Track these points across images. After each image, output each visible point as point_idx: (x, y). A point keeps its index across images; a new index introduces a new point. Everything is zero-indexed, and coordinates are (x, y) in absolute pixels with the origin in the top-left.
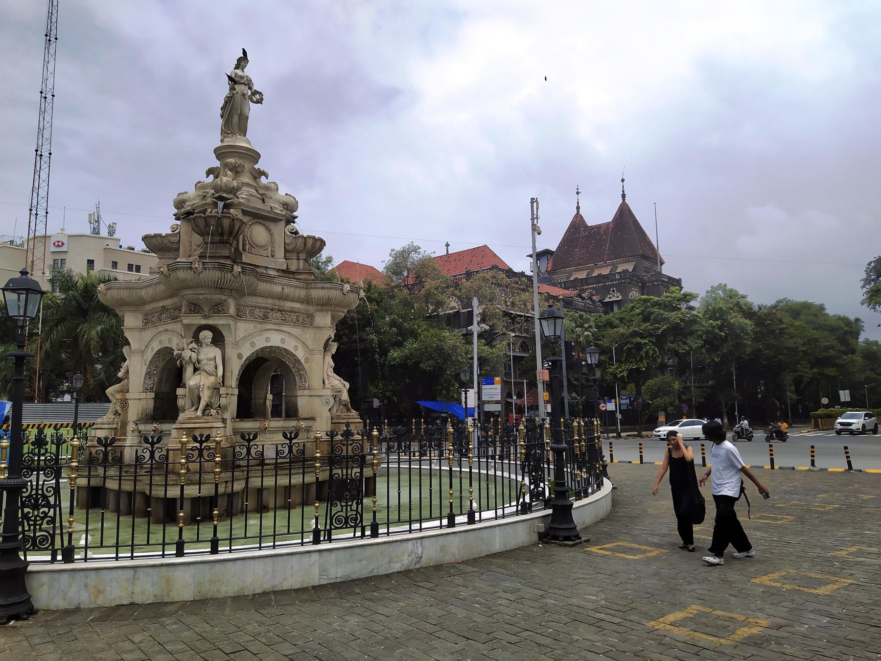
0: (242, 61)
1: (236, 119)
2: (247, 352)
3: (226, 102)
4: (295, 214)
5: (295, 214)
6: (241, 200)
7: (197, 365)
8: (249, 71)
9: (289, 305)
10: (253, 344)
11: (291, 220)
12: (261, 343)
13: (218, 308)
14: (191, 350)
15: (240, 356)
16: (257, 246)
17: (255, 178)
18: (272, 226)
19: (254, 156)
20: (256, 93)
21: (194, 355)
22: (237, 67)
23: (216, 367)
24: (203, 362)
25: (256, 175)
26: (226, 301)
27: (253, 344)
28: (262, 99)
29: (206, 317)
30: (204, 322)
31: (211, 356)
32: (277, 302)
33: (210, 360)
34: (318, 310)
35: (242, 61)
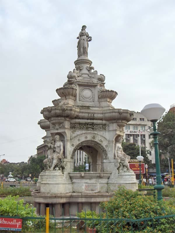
0: (84, 27)
1: (82, 50)
3: (78, 44)
4: (104, 82)
5: (104, 82)
7: (54, 149)
8: (87, 30)
9: (95, 121)
11: (103, 84)
12: (83, 139)
16: (86, 98)
17: (89, 71)
18: (92, 89)
21: (52, 146)
22: (82, 30)
23: (60, 150)
24: (56, 148)
25: (89, 69)
28: (91, 39)
30: (57, 131)
31: (58, 145)
33: (58, 147)
34: (110, 123)
35: (84, 27)
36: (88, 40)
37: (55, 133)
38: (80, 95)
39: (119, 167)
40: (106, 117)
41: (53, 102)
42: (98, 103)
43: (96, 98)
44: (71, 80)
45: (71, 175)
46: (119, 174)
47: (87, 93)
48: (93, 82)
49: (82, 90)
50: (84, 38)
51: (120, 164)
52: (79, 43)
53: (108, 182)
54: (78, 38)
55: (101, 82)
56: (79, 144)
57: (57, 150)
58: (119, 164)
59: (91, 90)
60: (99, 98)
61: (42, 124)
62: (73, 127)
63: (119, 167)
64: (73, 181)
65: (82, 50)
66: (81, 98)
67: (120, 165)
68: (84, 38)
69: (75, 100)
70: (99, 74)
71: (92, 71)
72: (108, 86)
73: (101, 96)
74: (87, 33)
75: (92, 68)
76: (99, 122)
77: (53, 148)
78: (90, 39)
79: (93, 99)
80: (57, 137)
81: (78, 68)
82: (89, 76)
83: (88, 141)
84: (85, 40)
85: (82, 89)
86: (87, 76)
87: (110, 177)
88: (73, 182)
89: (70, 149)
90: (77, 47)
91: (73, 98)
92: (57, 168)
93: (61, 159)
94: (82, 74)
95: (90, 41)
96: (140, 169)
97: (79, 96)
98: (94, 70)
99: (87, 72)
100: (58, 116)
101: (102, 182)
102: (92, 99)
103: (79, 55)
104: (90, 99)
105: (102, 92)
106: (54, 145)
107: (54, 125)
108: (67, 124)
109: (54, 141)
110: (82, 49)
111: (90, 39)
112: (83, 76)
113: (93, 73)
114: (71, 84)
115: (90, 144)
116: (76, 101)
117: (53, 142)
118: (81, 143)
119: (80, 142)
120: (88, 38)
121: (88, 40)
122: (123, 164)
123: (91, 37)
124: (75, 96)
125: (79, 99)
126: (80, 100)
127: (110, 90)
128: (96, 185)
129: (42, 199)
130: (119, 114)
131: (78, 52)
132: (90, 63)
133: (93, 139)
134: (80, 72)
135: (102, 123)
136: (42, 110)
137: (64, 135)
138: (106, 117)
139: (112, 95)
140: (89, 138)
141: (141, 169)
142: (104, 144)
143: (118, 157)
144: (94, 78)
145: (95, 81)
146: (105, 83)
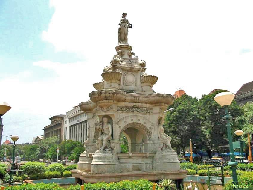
0: (124, 15)
1: (122, 35)
2: (123, 125)
3: (119, 30)
5: (145, 68)
6: (122, 65)
7: (103, 132)
8: (127, 18)
9: (140, 104)
10: (125, 122)
11: (144, 70)
12: (129, 121)
13: (109, 108)
14: (100, 125)
15: (120, 127)
16: (130, 82)
17: (130, 56)
18: (135, 74)
19: (130, 48)
20: (130, 24)
22: (123, 17)
23: (109, 132)
25: (130, 55)
26: (112, 105)
27: (125, 122)
28: (132, 26)
29: (105, 112)
32: (134, 104)
34: (153, 106)
35: (124, 15)
36: (129, 27)
37: (102, 115)
38: (124, 80)
39: (163, 148)
40: (150, 101)
41: (94, 85)
42: (140, 87)
43: (139, 82)
44: (115, 64)
45: (119, 155)
46: (162, 154)
47: (130, 78)
48: (136, 67)
49: (126, 75)
50: (124, 26)
51: (163, 144)
52: (120, 29)
53: (152, 162)
54: (120, 25)
55: (142, 67)
56: (125, 126)
57: (106, 132)
58: (162, 145)
59: (134, 76)
60: (141, 83)
61: (83, 106)
62: (120, 110)
63: (163, 148)
64: (121, 162)
65: (122, 35)
66: (125, 81)
67: (163, 146)
68: (124, 26)
69: (119, 84)
70: (140, 60)
71: (133, 56)
72: (149, 72)
73: (143, 80)
74: (128, 21)
75: (133, 54)
76: (145, 105)
77: (101, 130)
78: (131, 26)
79: (135, 84)
80: (105, 120)
81: (121, 54)
82: (130, 61)
83: (133, 123)
84: (126, 27)
85: (126, 74)
86: (129, 61)
87: (154, 157)
88: (121, 163)
89: (117, 131)
90: (118, 33)
91: (118, 82)
92: (107, 150)
93: (110, 140)
94: (125, 59)
95: (131, 27)
96: (240, 154)
97: (123, 80)
98: (134, 55)
99: (129, 58)
100: (107, 99)
101: (147, 161)
102: (134, 83)
103: (120, 40)
104: (133, 83)
105: (145, 76)
106: (103, 127)
107: (102, 108)
108: (115, 108)
109: (102, 123)
110: (122, 36)
111: (131, 26)
112: (125, 61)
113: (134, 59)
114: (116, 68)
115: (135, 126)
116: (120, 85)
117: (102, 124)
118: (128, 125)
119: (126, 124)
120: (128, 25)
121: (129, 27)
122: (166, 144)
123: (131, 24)
124: (120, 80)
125: (123, 83)
126: (123, 84)
127: (152, 76)
128: (142, 165)
129: (95, 179)
130: (163, 98)
131: (119, 38)
132: (130, 48)
133: (138, 122)
134: (122, 57)
135: (142, 106)
136: (90, 93)
137: (113, 119)
138: (150, 101)
139: (153, 79)
140: (135, 120)
141: (241, 154)
142: (148, 126)
143: (161, 138)
144: (135, 63)
145: (137, 66)
146: (146, 69)
